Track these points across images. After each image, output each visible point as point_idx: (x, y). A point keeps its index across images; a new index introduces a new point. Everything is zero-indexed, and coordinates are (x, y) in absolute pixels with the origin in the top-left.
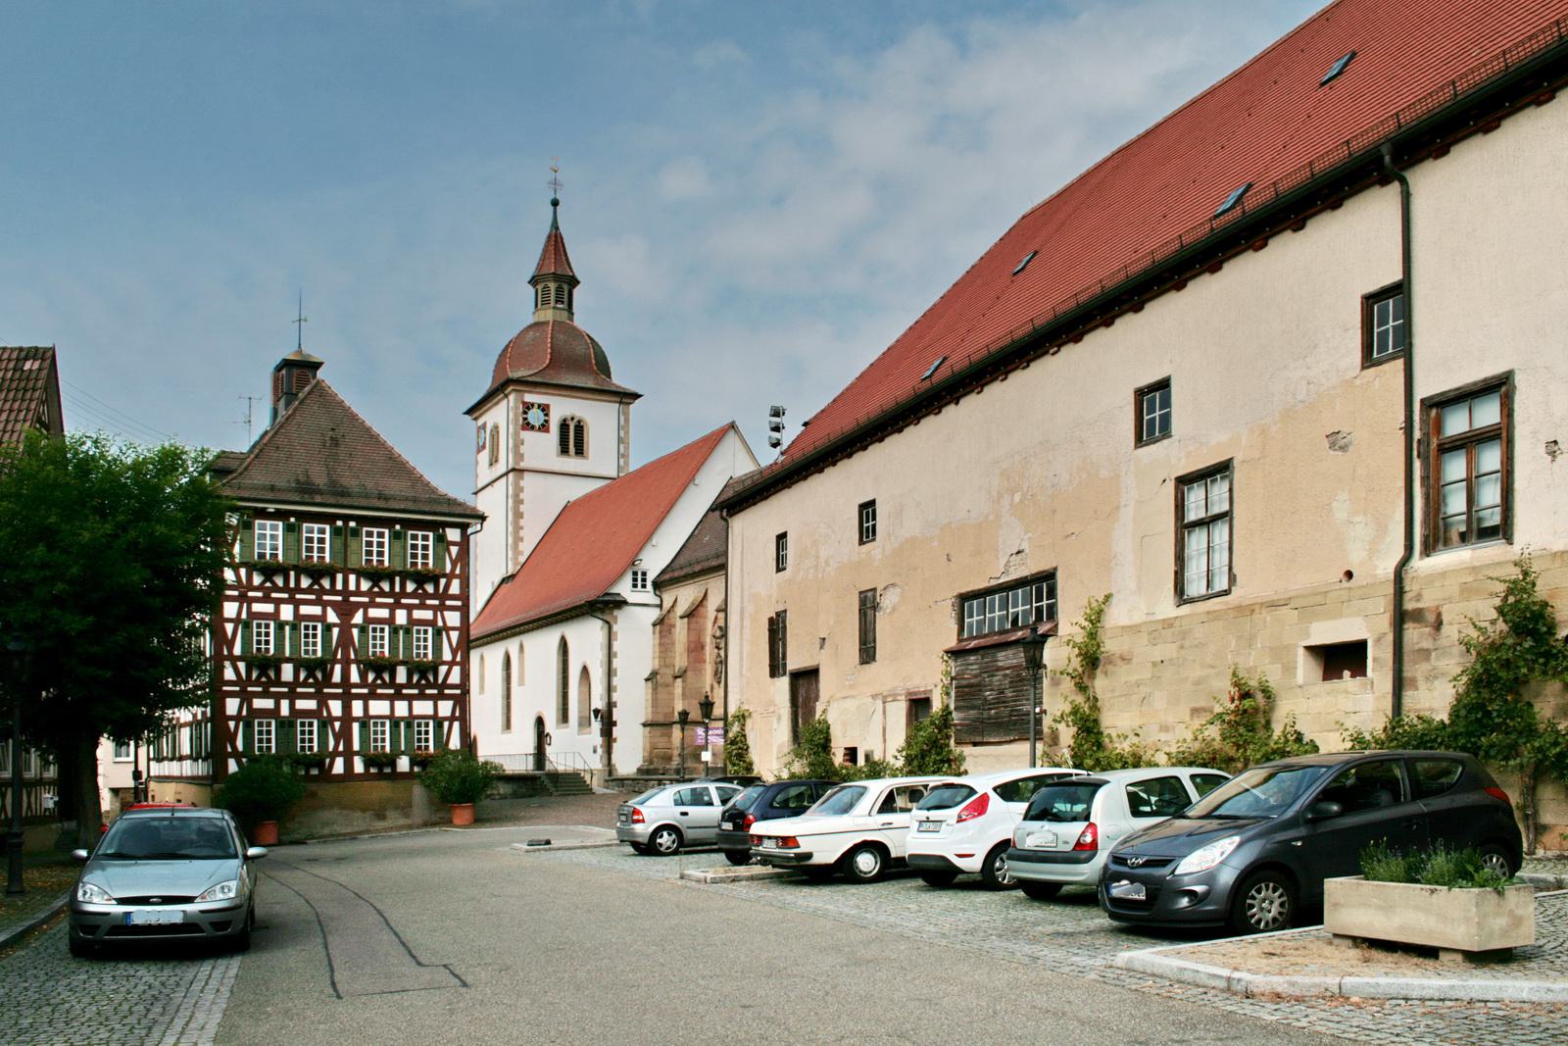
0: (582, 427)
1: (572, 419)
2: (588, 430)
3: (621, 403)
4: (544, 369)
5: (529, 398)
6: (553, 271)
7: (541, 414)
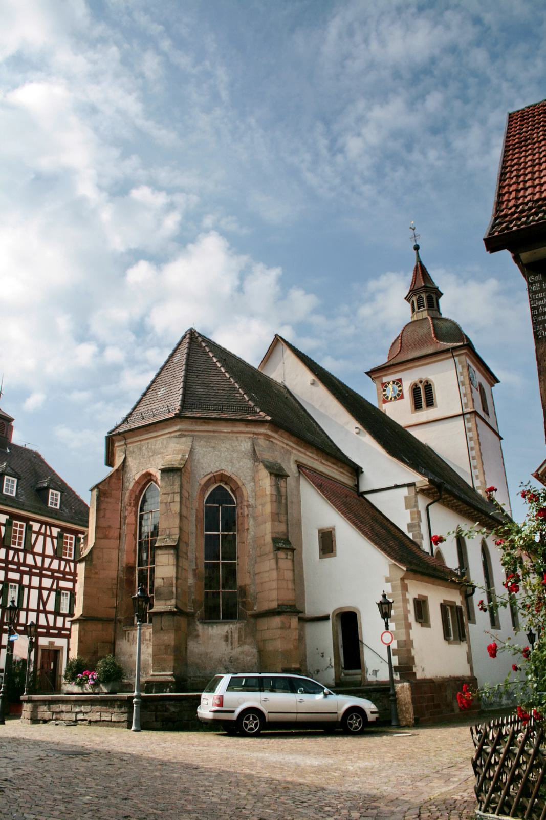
0: (430, 385)
1: (421, 382)
3: (453, 357)
5: (385, 380)
6: (423, 285)
7: (396, 387)
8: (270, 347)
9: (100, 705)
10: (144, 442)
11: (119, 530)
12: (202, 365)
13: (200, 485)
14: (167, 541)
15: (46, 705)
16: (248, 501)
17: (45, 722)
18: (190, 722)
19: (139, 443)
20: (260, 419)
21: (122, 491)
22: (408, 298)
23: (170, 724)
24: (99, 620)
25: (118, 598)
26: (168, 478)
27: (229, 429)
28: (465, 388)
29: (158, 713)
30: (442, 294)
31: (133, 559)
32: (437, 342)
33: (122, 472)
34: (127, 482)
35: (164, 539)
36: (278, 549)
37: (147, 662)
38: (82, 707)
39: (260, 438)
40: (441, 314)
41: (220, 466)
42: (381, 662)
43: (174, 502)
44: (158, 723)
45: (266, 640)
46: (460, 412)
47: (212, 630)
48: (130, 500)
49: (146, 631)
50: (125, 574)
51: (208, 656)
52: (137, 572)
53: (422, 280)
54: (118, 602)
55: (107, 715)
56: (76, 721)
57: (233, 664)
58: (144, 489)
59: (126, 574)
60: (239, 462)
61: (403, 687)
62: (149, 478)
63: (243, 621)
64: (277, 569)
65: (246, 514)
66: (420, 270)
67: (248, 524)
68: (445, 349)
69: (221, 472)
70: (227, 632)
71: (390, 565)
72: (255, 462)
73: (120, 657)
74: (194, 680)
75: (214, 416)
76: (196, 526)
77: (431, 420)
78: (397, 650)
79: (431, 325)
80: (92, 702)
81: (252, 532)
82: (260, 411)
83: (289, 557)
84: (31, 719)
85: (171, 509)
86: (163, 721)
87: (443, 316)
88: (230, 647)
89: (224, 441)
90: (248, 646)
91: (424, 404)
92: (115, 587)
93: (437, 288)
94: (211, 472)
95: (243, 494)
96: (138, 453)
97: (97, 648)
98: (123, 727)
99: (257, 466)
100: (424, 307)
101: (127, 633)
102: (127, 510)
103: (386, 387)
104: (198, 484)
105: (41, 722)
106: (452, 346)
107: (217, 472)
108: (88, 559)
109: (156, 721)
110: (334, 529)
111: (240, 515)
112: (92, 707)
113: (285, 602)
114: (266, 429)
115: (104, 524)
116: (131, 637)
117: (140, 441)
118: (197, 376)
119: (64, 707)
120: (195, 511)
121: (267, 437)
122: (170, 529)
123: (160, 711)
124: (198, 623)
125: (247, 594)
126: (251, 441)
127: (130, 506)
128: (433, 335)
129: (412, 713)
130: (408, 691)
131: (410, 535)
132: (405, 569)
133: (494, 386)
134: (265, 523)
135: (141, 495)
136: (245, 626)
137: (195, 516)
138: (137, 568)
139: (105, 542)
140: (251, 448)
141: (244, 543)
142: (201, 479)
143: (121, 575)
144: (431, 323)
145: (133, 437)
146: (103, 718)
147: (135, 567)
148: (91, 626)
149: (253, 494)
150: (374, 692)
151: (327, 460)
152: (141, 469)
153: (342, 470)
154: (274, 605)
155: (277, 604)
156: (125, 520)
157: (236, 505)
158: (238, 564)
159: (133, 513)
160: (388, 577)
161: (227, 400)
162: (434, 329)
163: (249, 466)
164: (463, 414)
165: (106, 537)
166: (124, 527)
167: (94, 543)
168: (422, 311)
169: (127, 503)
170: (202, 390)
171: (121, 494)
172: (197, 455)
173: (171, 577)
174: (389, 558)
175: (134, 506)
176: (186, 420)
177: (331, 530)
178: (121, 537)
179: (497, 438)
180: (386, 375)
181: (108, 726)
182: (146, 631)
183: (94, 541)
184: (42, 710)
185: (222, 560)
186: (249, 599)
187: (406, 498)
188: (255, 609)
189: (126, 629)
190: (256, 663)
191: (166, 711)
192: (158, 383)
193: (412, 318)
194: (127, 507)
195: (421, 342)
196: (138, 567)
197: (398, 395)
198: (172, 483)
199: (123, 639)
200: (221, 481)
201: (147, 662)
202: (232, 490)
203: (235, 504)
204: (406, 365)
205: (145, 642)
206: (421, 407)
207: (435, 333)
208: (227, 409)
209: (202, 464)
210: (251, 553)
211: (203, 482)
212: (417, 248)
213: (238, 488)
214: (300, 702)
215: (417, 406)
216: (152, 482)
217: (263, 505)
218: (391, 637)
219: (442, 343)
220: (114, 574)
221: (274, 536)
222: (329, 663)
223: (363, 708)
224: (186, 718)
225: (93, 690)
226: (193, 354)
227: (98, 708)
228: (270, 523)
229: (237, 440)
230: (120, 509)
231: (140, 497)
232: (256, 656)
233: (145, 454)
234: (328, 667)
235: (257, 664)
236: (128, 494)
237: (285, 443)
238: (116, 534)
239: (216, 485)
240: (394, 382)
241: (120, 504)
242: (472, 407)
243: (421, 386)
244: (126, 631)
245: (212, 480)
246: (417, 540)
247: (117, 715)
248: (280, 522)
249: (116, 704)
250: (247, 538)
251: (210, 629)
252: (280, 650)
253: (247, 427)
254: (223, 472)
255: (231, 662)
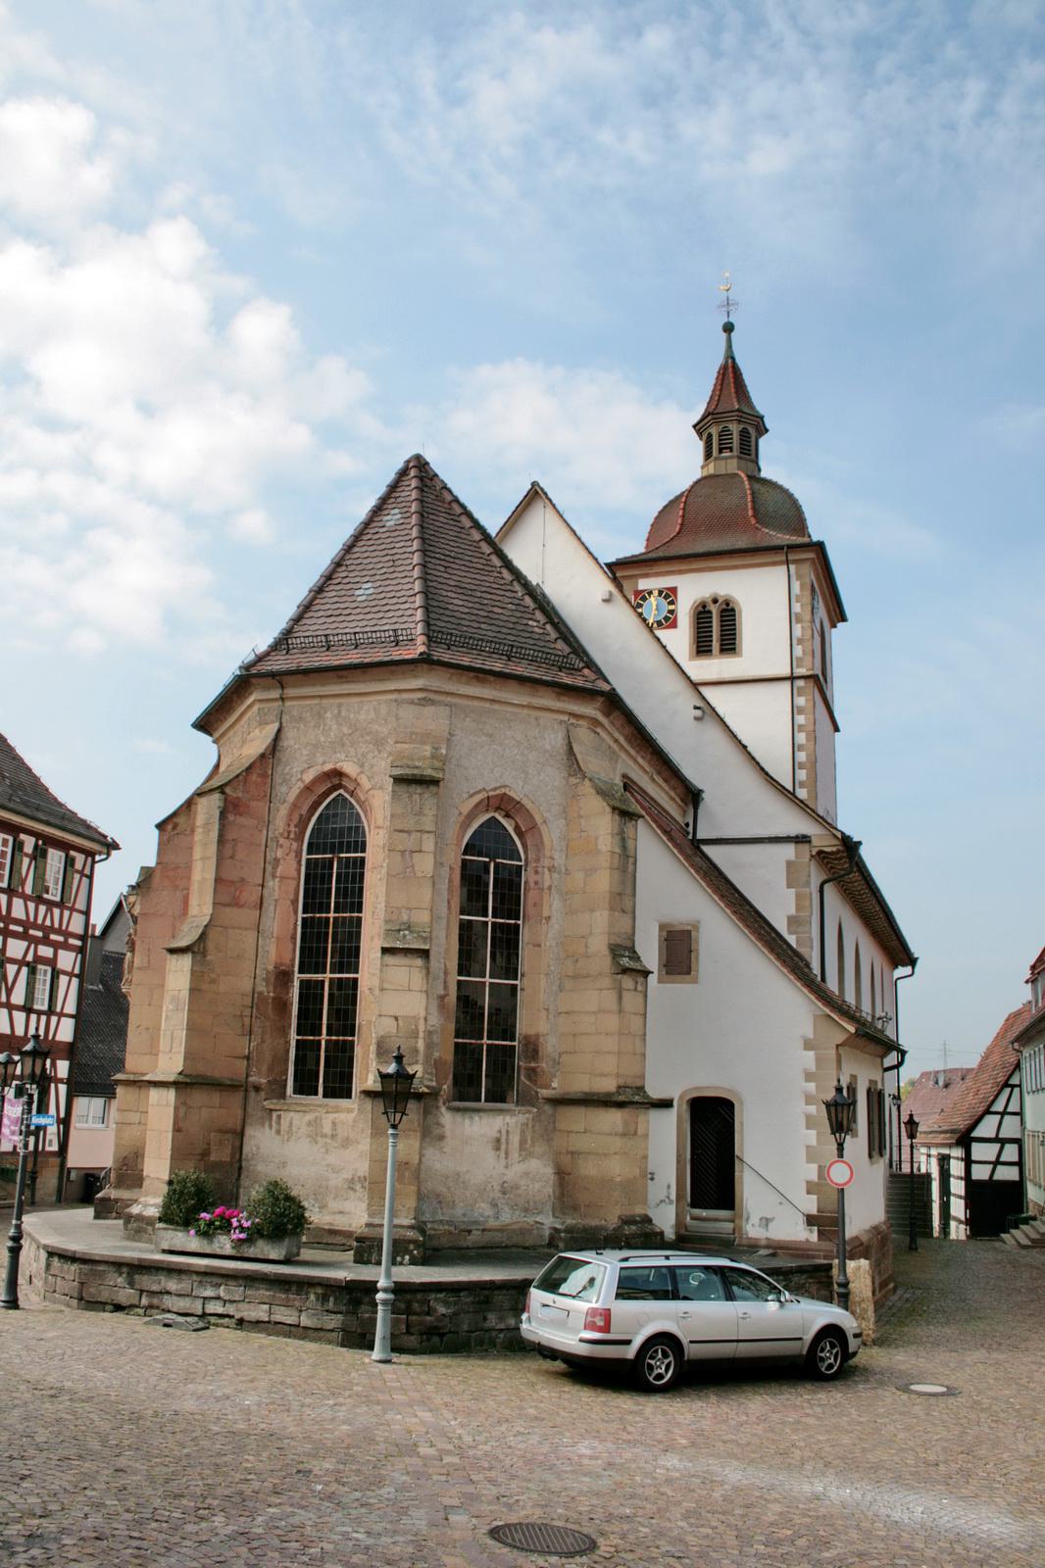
0: (733, 610)
1: (715, 601)
2: (741, 611)
3: (787, 563)
4: (672, 539)
5: (644, 584)
7: (664, 602)
8: (517, 507)
9: (267, 1290)
10: (331, 701)
11: (260, 888)
12: (451, 543)
13: (460, 813)
14: (405, 936)
15: (120, 1274)
16: (552, 858)
17: (118, 1308)
18: (473, 1335)
19: (317, 701)
20: (589, 685)
21: (270, 802)
22: (699, 428)
23: (436, 1339)
24: (219, 1085)
25: (253, 1037)
26: (410, 796)
27: (525, 700)
28: (802, 627)
29: (414, 1318)
30: (767, 431)
31: (290, 956)
32: (757, 528)
33: (271, 760)
34: (281, 784)
35: (399, 930)
36: (625, 971)
37: (324, 1183)
38: (222, 1287)
39: (581, 726)
40: (759, 470)
41: (501, 777)
42: (781, 1203)
43: (420, 851)
44: (413, 1338)
45: (580, 1154)
46: (786, 672)
47: (471, 1125)
48: (289, 825)
49: (324, 1116)
50: (271, 988)
51: (461, 1180)
52: (296, 984)
53: (734, 395)
54: (252, 1044)
55: (289, 1312)
56: (204, 1315)
57: (507, 1196)
58: (320, 804)
59: (275, 988)
60: (539, 773)
61: (859, 1268)
62: (336, 781)
63: (530, 1108)
64: (620, 1011)
65: (546, 885)
66: (731, 375)
67: (550, 906)
68: (772, 544)
69: (503, 790)
70: (500, 1132)
71: (814, 1015)
72: (570, 775)
73: (255, 1165)
74: (435, 1230)
75: (498, 666)
76: (449, 902)
77: (727, 680)
78: (817, 1184)
79: (749, 492)
80: (250, 1279)
81: (555, 925)
82: (583, 668)
83: (640, 988)
84: (81, 1299)
85: (413, 866)
86: (421, 1334)
87: (763, 474)
88: (503, 1162)
89: (512, 724)
90: (538, 1161)
91: (716, 645)
92: (247, 1012)
93: (762, 418)
94: (484, 789)
95: (542, 842)
96: (313, 724)
97: (209, 1144)
98: (330, 1342)
99: (576, 785)
100: (731, 451)
101: (275, 1114)
102: (281, 846)
103: (644, 599)
104: (457, 812)
105: (111, 1307)
106: (790, 542)
107: (495, 789)
108: (196, 949)
109: (408, 1332)
110: (696, 927)
111: (532, 885)
112: (248, 1292)
113: (630, 1082)
114: (595, 709)
115: (232, 874)
116: (284, 1123)
117: (320, 697)
118: (446, 567)
119: (172, 1285)
120: (448, 869)
121: (595, 722)
122: (408, 908)
123: (416, 1314)
124: (443, 1109)
125: (540, 1053)
126: (565, 730)
127: (288, 838)
128: (750, 513)
129: (873, 1319)
130: (867, 1276)
131: (792, 940)
132: (852, 1030)
133: (835, 627)
134: (592, 911)
135: (313, 815)
136: (533, 1120)
137: (447, 881)
138: (296, 975)
139: (231, 914)
140: (562, 745)
141: (539, 946)
142: (463, 802)
143: (261, 987)
144: (747, 487)
145: (302, 686)
146: (277, 1318)
147: (293, 972)
148: (198, 1097)
149: (563, 843)
150: (796, 1272)
151: (666, 781)
152: (321, 760)
153: (672, 794)
154: (607, 1085)
155: (615, 1085)
156: (275, 868)
157: (522, 863)
158: (522, 989)
159: (293, 854)
160: (809, 1039)
161: (513, 632)
162: (753, 502)
163: (557, 783)
164: (792, 678)
165: (236, 903)
166: (271, 883)
167: (212, 915)
168: (726, 458)
169: (281, 831)
170: (461, 603)
171: (267, 809)
172: (458, 748)
173: (415, 1017)
174: (820, 1004)
175: (295, 840)
176: (441, 671)
177: (689, 928)
178: (265, 905)
179: (831, 728)
180: (646, 576)
181: (289, 1335)
182: (324, 1116)
183: (208, 910)
184: (111, 1283)
185: (490, 977)
186: (544, 1065)
187: (789, 864)
188: (554, 1085)
189: (272, 1107)
190: (549, 1196)
191: (428, 1314)
192: (350, 568)
193: (703, 467)
194: (282, 841)
195: (724, 522)
196: (300, 973)
197: (666, 619)
198: (417, 808)
199: (263, 1125)
200: (498, 809)
201: (324, 1183)
202: (517, 829)
203: (521, 861)
204: (690, 562)
205: (319, 1138)
206: (711, 651)
207: (754, 508)
208: (546, 659)
209: (466, 769)
210: (552, 968)
211: (466, 809)
212: (729, 328)
213: (534, 827)
214: (743, 1318)
215: (702, 648)
216: (341, 791)
217: (590, 871)
218: (849, 1172)
219: (767, 531)
220: (246, 985)
221: (612, 942)
222: (666, 1194)
223: (842, 1326)
224: (466, 1327)
225: (238, 1251)
226: (431, 516)
227: (264, 1293)
228: (606, 913)
229: (538, 725)
230: (264, 842)
231: (309, 820)
232: (551, 1182)
233: (330, 729)
234: (661, 1202)
235: (552, 1198)
236: (282, 813)
237: (613, 737)
238: (255, 897)
239: (488, 816)
240: (660, 593)
241: (265, 832)
242: (811, 666)
243: (714, 609)
244: (271, 1110)
245: (483, 807)
246: (802, 950)
247: (313, 1315)
248: (624, 911)
249: (312, 1290)
250: (546, 937)
251: (467, 1121)
252: (618, 1179)
253: (559, 700)
254: (507, 792)
255: (504, 1193)
